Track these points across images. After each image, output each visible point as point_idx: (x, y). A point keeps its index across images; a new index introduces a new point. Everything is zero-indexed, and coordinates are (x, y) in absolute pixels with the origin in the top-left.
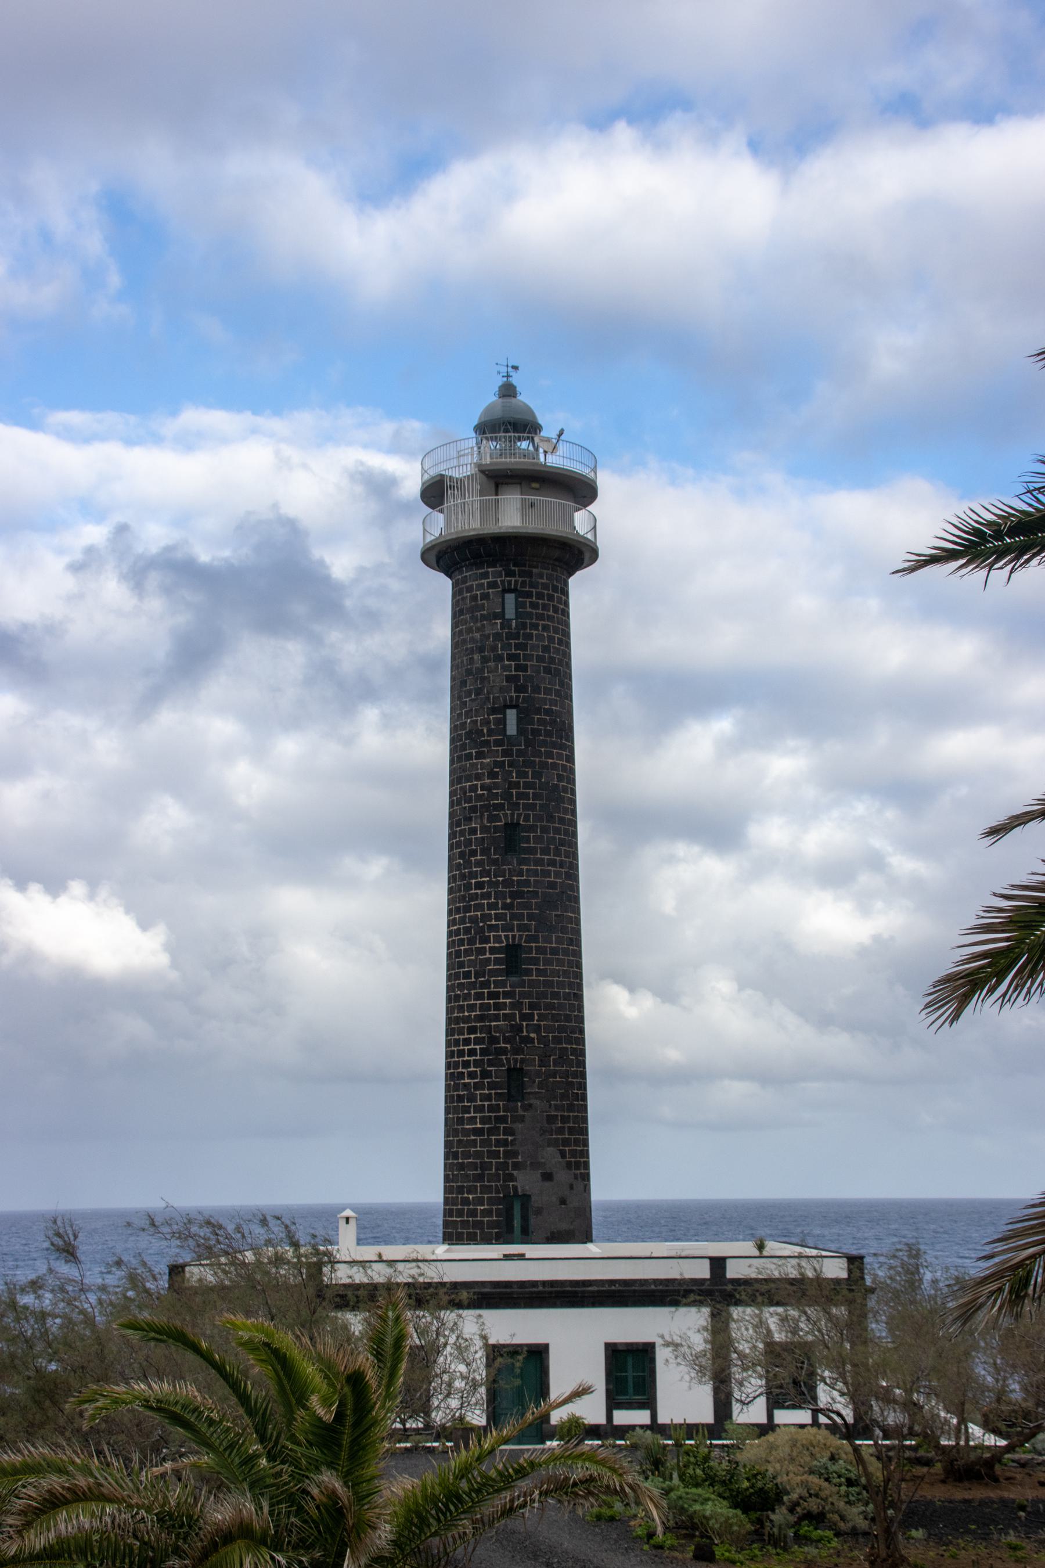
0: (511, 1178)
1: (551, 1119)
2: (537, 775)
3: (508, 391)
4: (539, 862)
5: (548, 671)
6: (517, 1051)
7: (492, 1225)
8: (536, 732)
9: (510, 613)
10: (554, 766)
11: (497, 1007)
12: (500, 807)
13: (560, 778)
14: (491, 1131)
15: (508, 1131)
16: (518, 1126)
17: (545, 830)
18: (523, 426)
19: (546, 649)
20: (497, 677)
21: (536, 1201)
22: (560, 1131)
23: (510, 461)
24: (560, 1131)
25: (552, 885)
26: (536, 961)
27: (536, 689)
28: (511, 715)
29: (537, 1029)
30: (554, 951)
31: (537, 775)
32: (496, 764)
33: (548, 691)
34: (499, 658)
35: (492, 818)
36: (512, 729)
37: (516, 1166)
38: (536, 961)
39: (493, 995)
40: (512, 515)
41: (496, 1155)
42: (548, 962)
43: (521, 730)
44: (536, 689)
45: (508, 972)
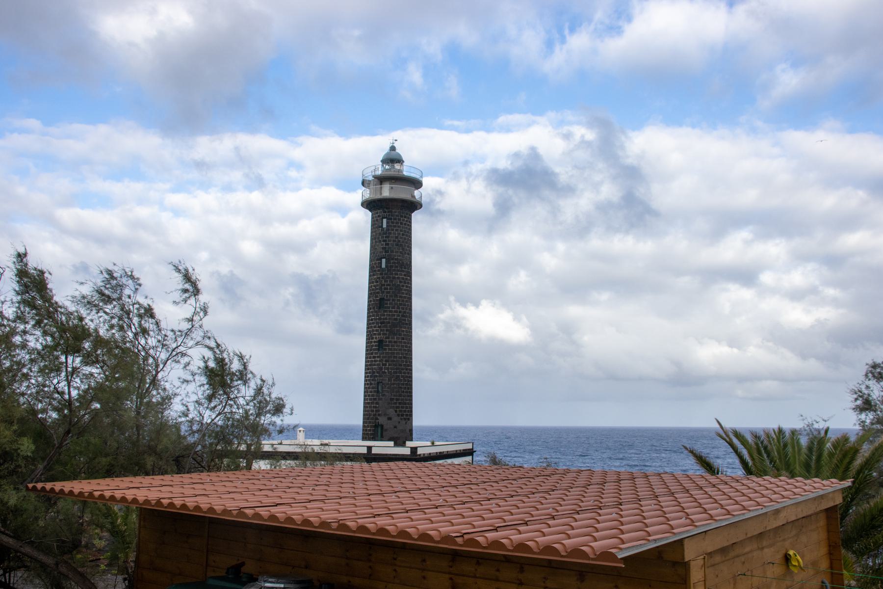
0: (377, 419)
1: (392, 399)
2: (391, 281)
3: (393, 148)
4: (390, 311)
5: (397, 245)
6: (380, 376)
7: (371, 434)
8: (391, 267)
9: (385, 226)
10: (398, 278)
11: (375, 361)
12: (378, 293)
13: (401, 282)
14: (372, 403)
15: (377, 403)
16: (380, 402)
17: (393, 300)
18: (400, 161)
19: (397, 237)
20: (379, 248)
21: (385, 427)
22: (396, 403)
23: (392, 173)
24: (396, 403)
25: (396, 319)
26: (388, 346)
27: (392, 252)
28: (384, 261)
29: (388, 369)
30: (395, 342)
31: (391, 281)
32: (379, 278)
33: (397, 252)
34: (380, 241)
35: (376, 297)
36: (383, 266)
37: (379, 415)
38: (388, 346)
39: (374, 357)
40: (386, 192)
41: (372, 411)
42: (393, 346)
43: (386, 266)
44: (392, 252)
45: (379, 350)
